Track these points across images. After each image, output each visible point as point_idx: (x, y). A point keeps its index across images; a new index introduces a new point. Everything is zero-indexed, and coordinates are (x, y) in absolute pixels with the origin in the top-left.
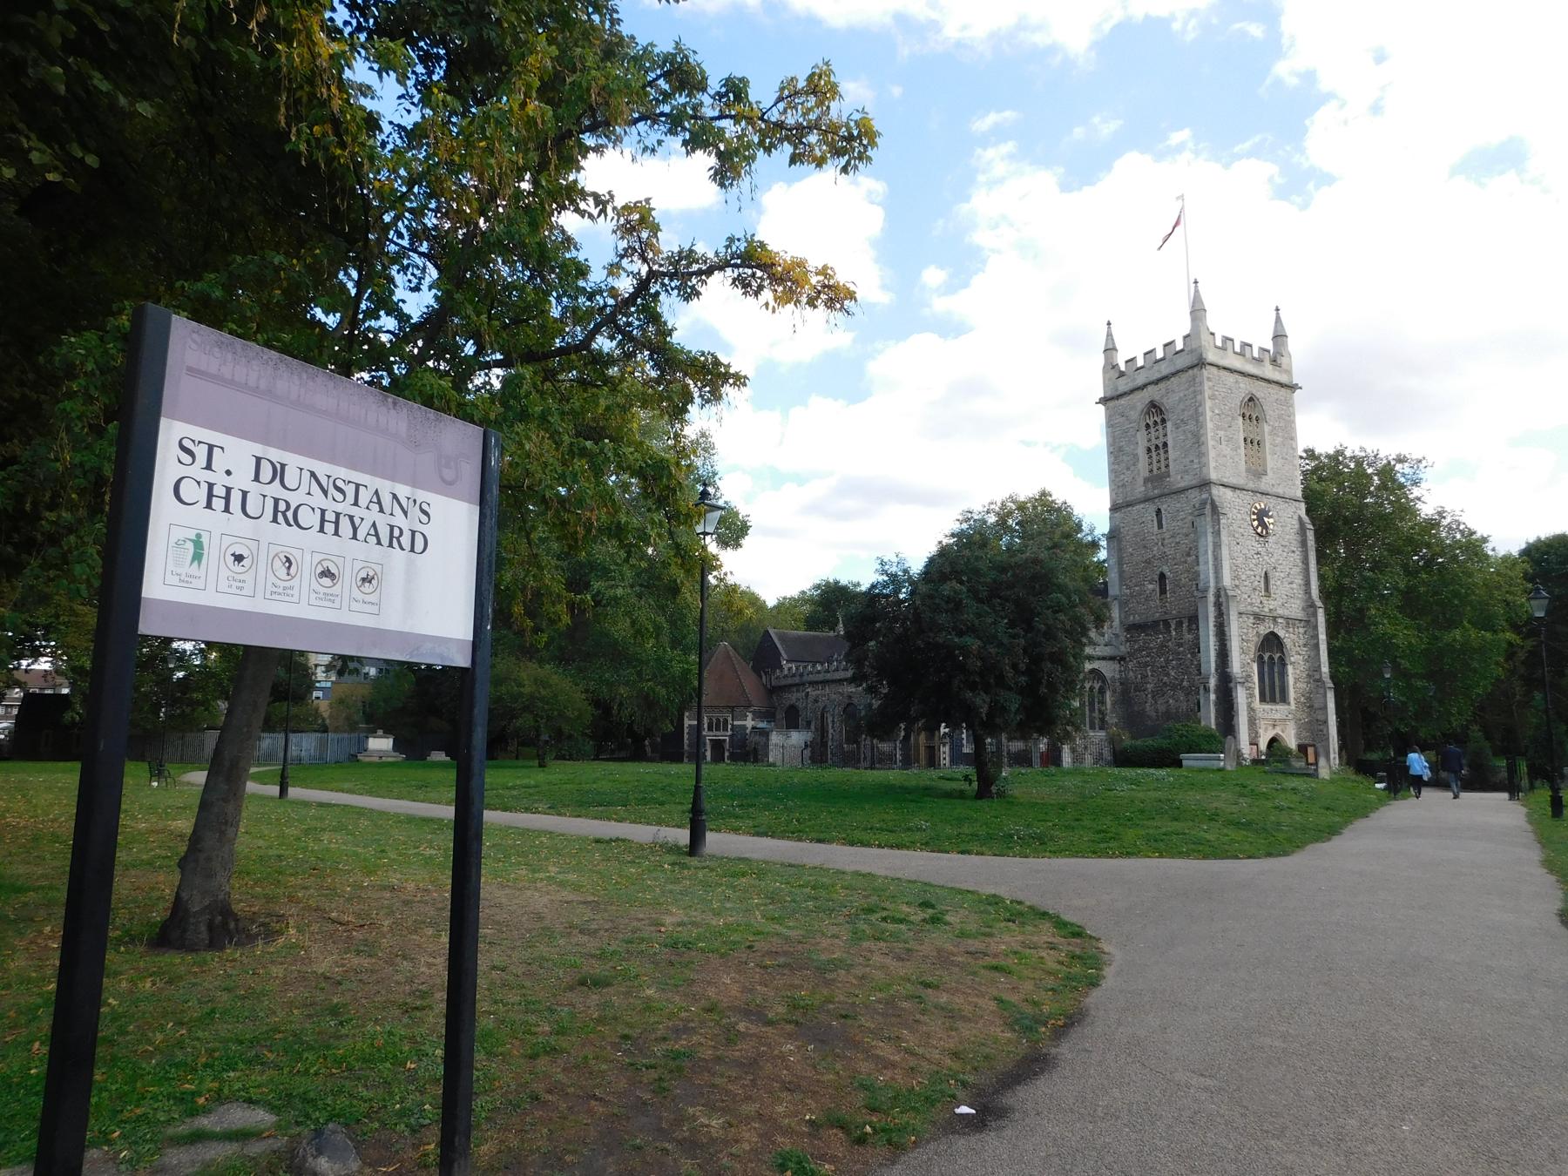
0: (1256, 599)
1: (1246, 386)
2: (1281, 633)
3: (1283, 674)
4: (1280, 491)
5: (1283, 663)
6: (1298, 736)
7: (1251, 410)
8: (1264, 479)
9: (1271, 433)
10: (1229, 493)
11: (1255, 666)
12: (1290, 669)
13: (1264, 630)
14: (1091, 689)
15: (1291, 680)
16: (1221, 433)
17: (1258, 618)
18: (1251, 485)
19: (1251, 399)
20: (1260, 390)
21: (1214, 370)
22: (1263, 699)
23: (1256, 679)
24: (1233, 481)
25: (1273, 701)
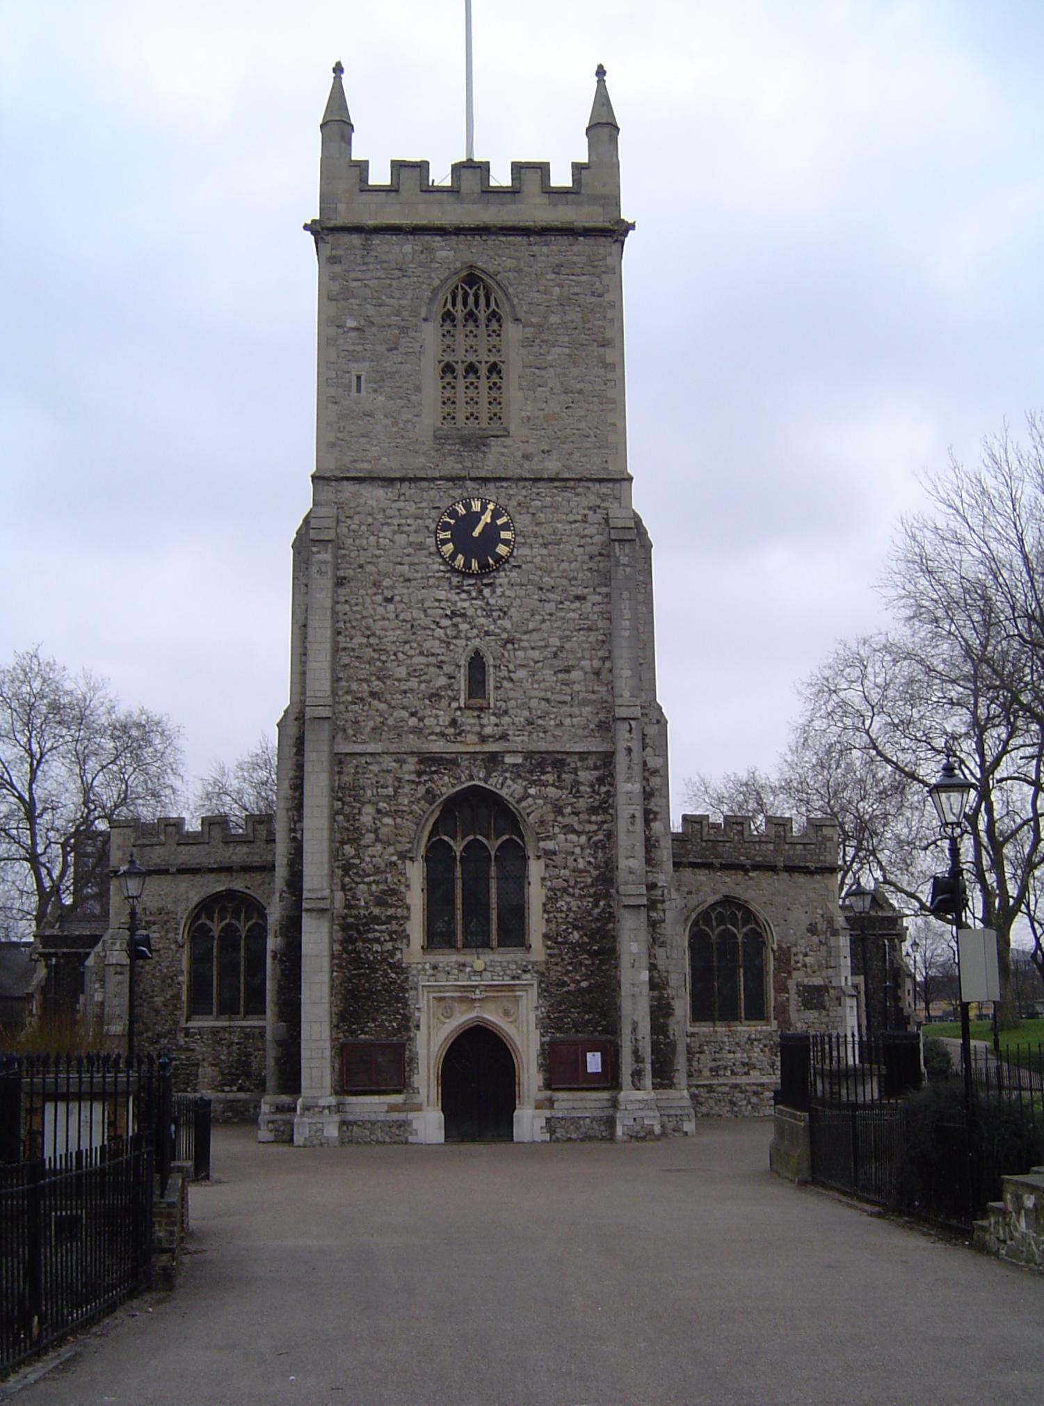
0: (439, 718)
1: (447, 253)
2: (510, 790)
3: (521, 880)
4: (552, 466)
5: (515, 855)
6: (547, 1024)
7: (473, 299)
8: (495, 447)
9: (528, 343)
10: (375, 496)
11: (416, 873)
12: (536, 869)
13: (447, 786)
14: (230, 931)
15: (536, 895)
16: (361, 368)
17: (430, 761)
18: (451, 466)
19: (472, 279)
20: (480, 254)
21: (356, 239)
22: (437, 938)
23: (416, 898)
24: (391, 464)
25: (478, 941)
